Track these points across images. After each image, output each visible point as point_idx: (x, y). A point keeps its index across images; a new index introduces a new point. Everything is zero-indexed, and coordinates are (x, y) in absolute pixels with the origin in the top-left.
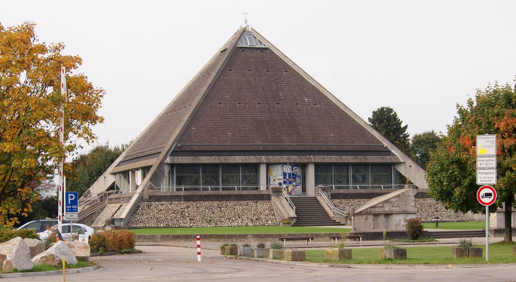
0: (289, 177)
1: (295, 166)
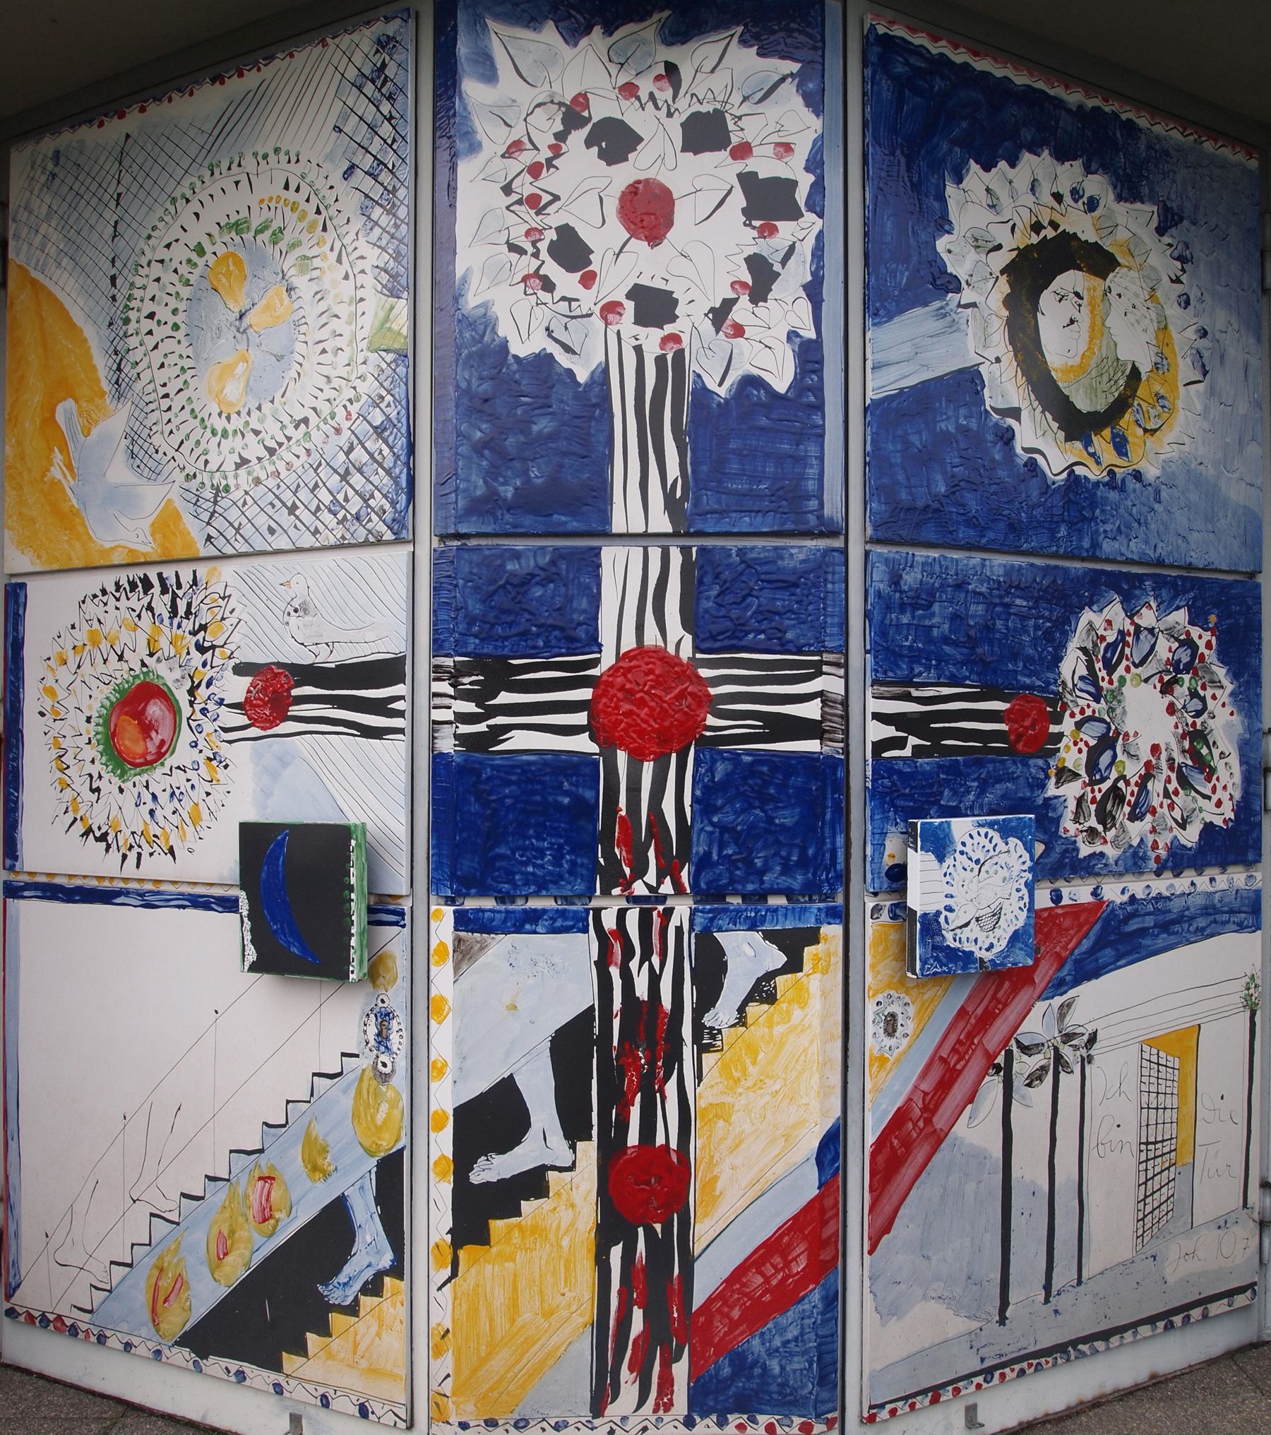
0: (740, 603)
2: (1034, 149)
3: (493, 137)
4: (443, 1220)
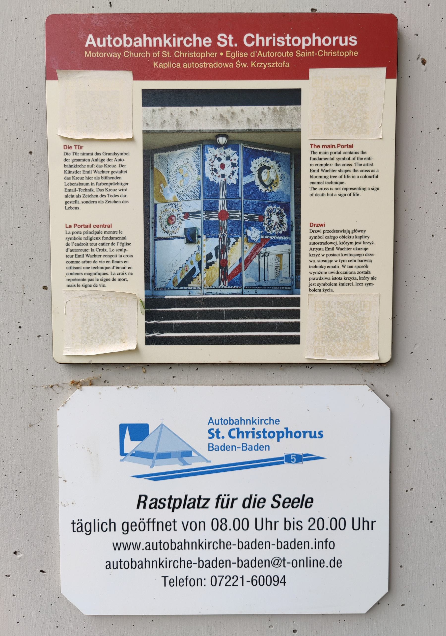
0: (232, 206)
1: (257, 155)
2: (261, 157)
3: (208, 159)
4: (205, 266)
